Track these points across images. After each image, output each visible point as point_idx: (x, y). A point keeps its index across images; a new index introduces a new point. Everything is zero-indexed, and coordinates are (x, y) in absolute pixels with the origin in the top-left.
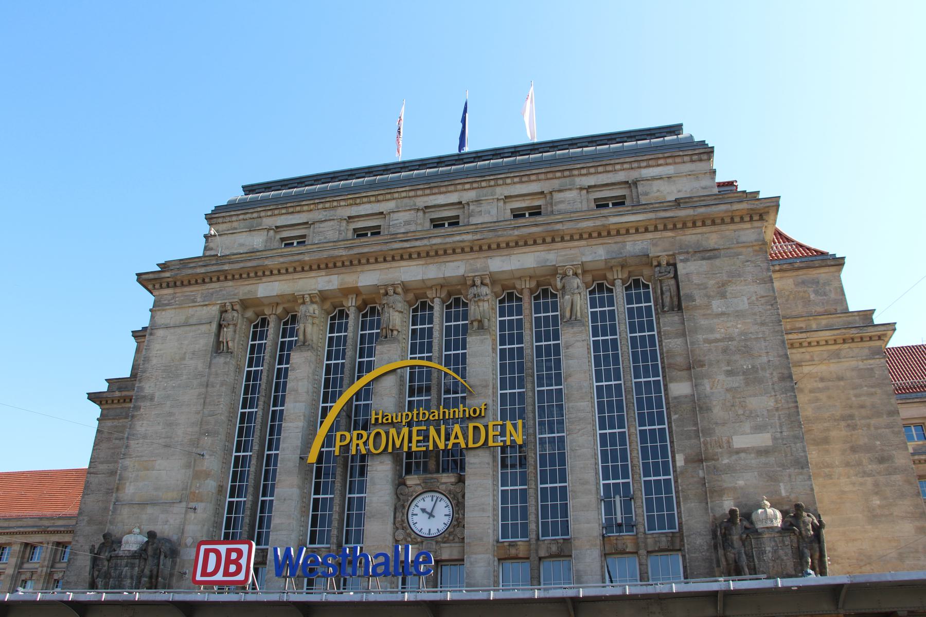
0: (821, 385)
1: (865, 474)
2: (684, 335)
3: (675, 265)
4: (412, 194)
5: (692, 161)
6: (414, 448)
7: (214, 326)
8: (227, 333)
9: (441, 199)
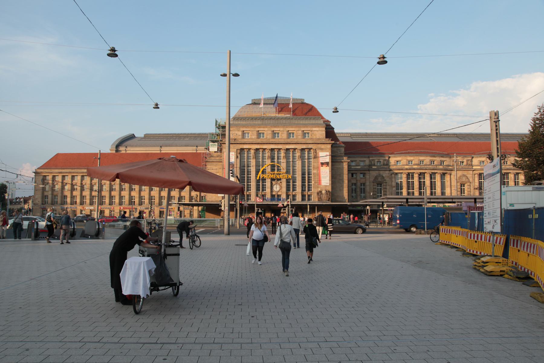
6: (274, 178)
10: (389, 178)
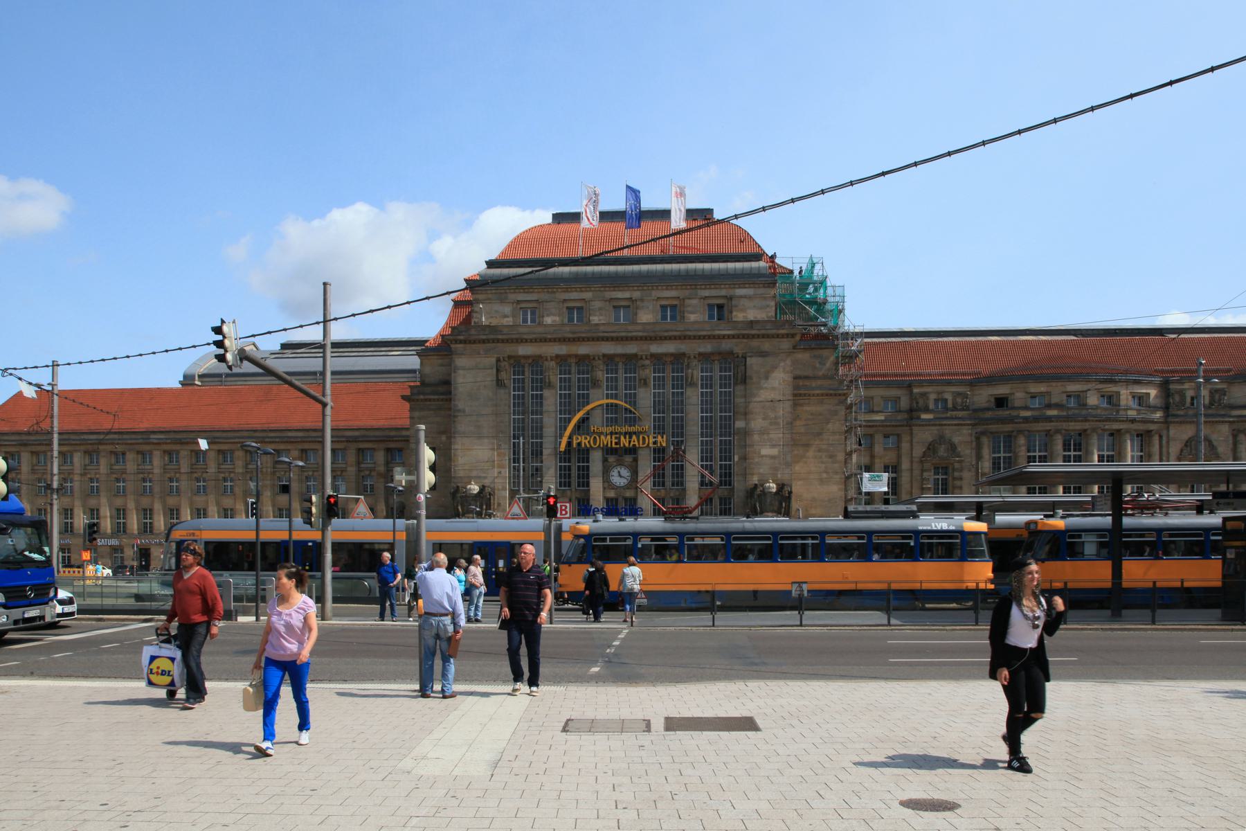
0: (810, 417)
1: (822, 462)
2: (745, 396)
3: (745, 358)
4: (602, 289)
5: (764, 287)
6: (614, 446)
7: (495, 370)
8: (503, 375)
9: (620, 295)
10: (972, 449)
